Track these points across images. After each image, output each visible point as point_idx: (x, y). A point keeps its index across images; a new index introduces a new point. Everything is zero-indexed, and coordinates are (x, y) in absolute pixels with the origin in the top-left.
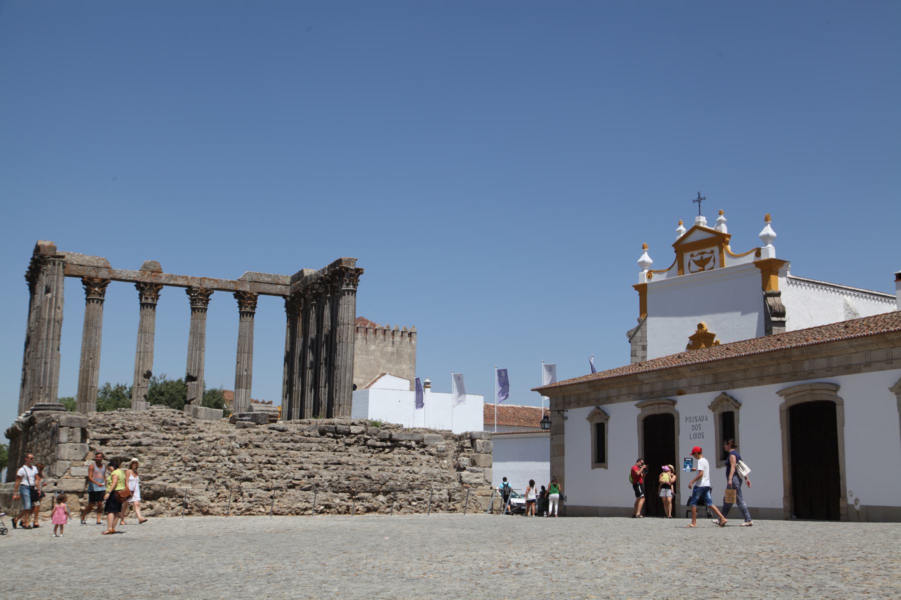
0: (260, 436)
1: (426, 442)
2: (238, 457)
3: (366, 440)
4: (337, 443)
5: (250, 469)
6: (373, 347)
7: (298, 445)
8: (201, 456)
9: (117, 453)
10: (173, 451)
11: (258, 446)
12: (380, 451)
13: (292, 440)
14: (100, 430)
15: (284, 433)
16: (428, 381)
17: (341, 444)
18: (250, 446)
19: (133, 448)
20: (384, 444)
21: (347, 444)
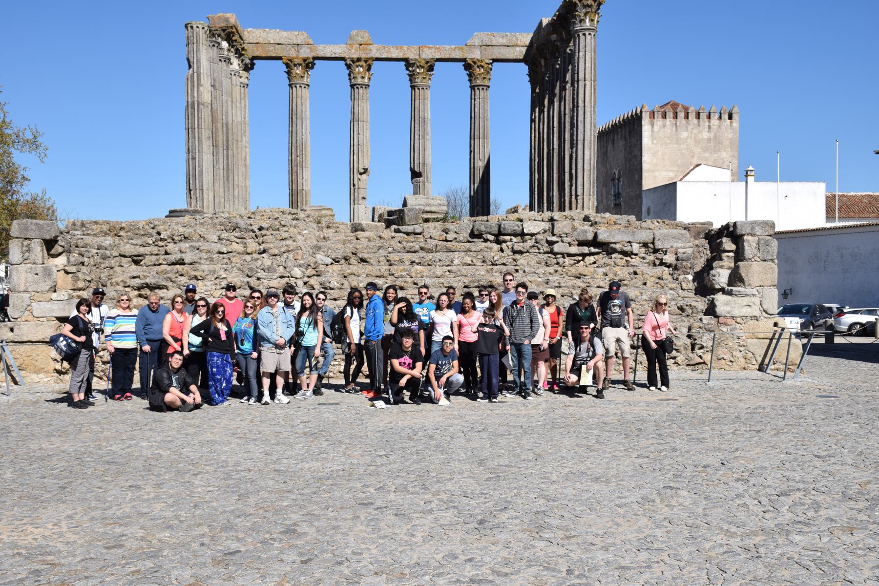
0: (373, 244)
1: (659, 245)
2: (320, 279)
3: (551, 243)
4: (502, 250)
5: (335, 300)
6: (684, 134)
7: (430, 256)
8: (258, 279)
9: (145, 277)
10: (214, 272)
11: (363, 260)
12: (579, 261)
13: (422, 249)
14: (139, 242)
15: (412, 237)
16: (751, 168)
17: (508, 252)
18: (353, 260)
19: (169, 268)
20: (586, 250)
21: (515, 252)
